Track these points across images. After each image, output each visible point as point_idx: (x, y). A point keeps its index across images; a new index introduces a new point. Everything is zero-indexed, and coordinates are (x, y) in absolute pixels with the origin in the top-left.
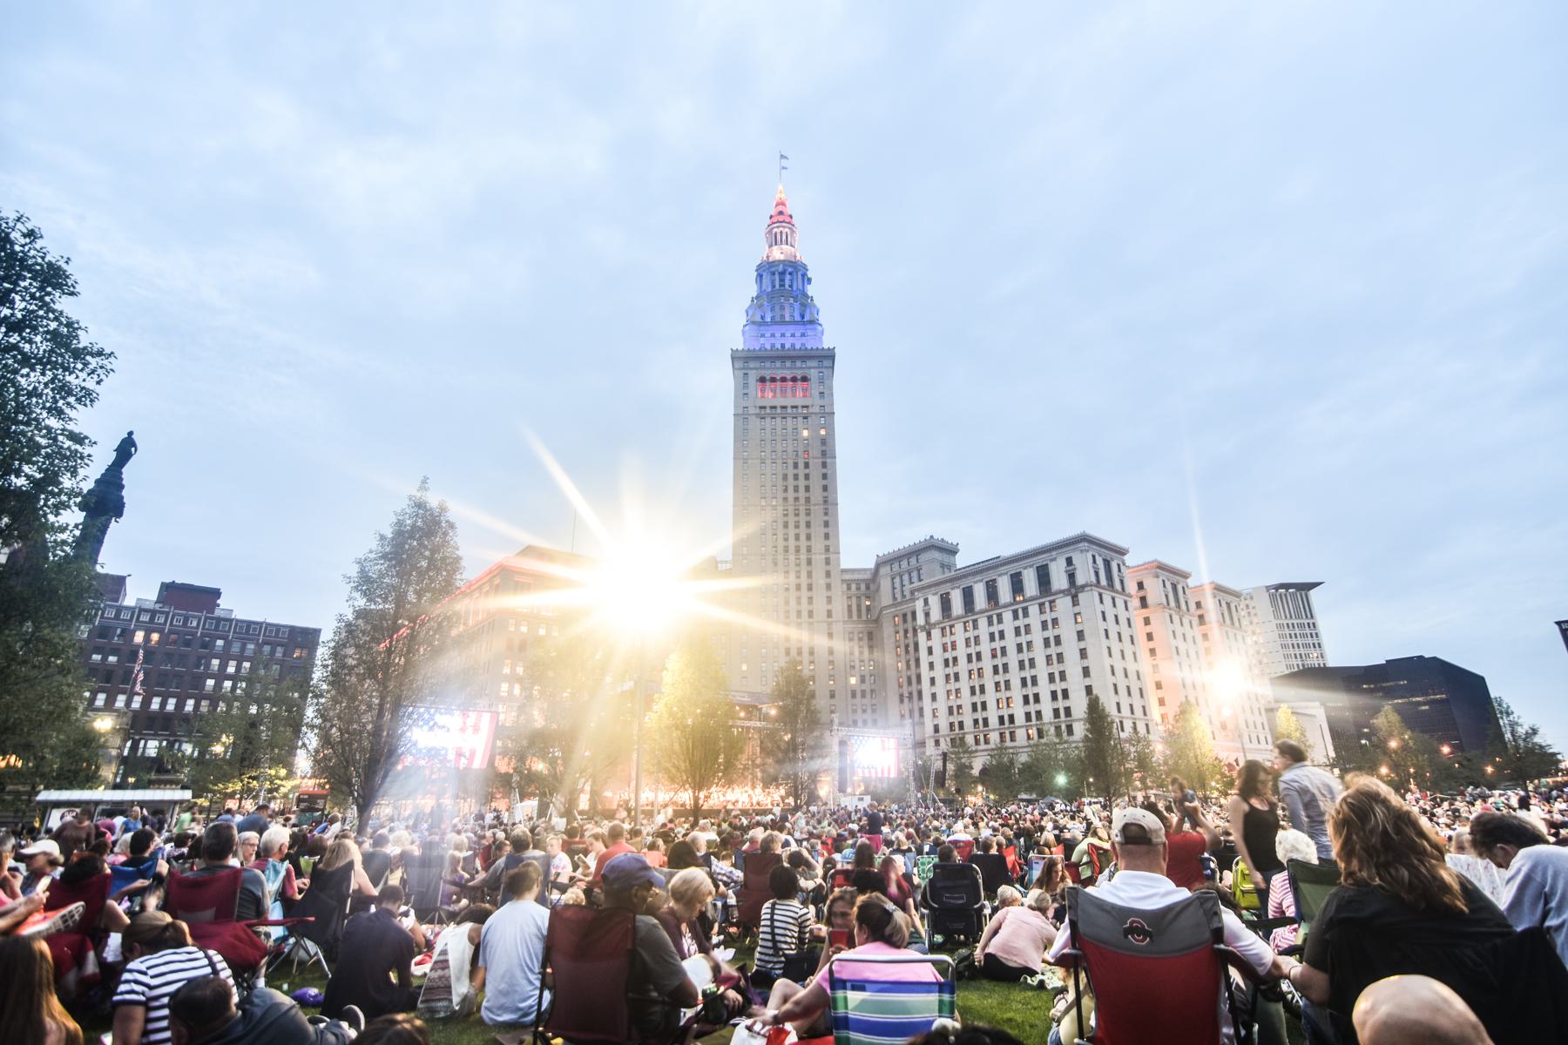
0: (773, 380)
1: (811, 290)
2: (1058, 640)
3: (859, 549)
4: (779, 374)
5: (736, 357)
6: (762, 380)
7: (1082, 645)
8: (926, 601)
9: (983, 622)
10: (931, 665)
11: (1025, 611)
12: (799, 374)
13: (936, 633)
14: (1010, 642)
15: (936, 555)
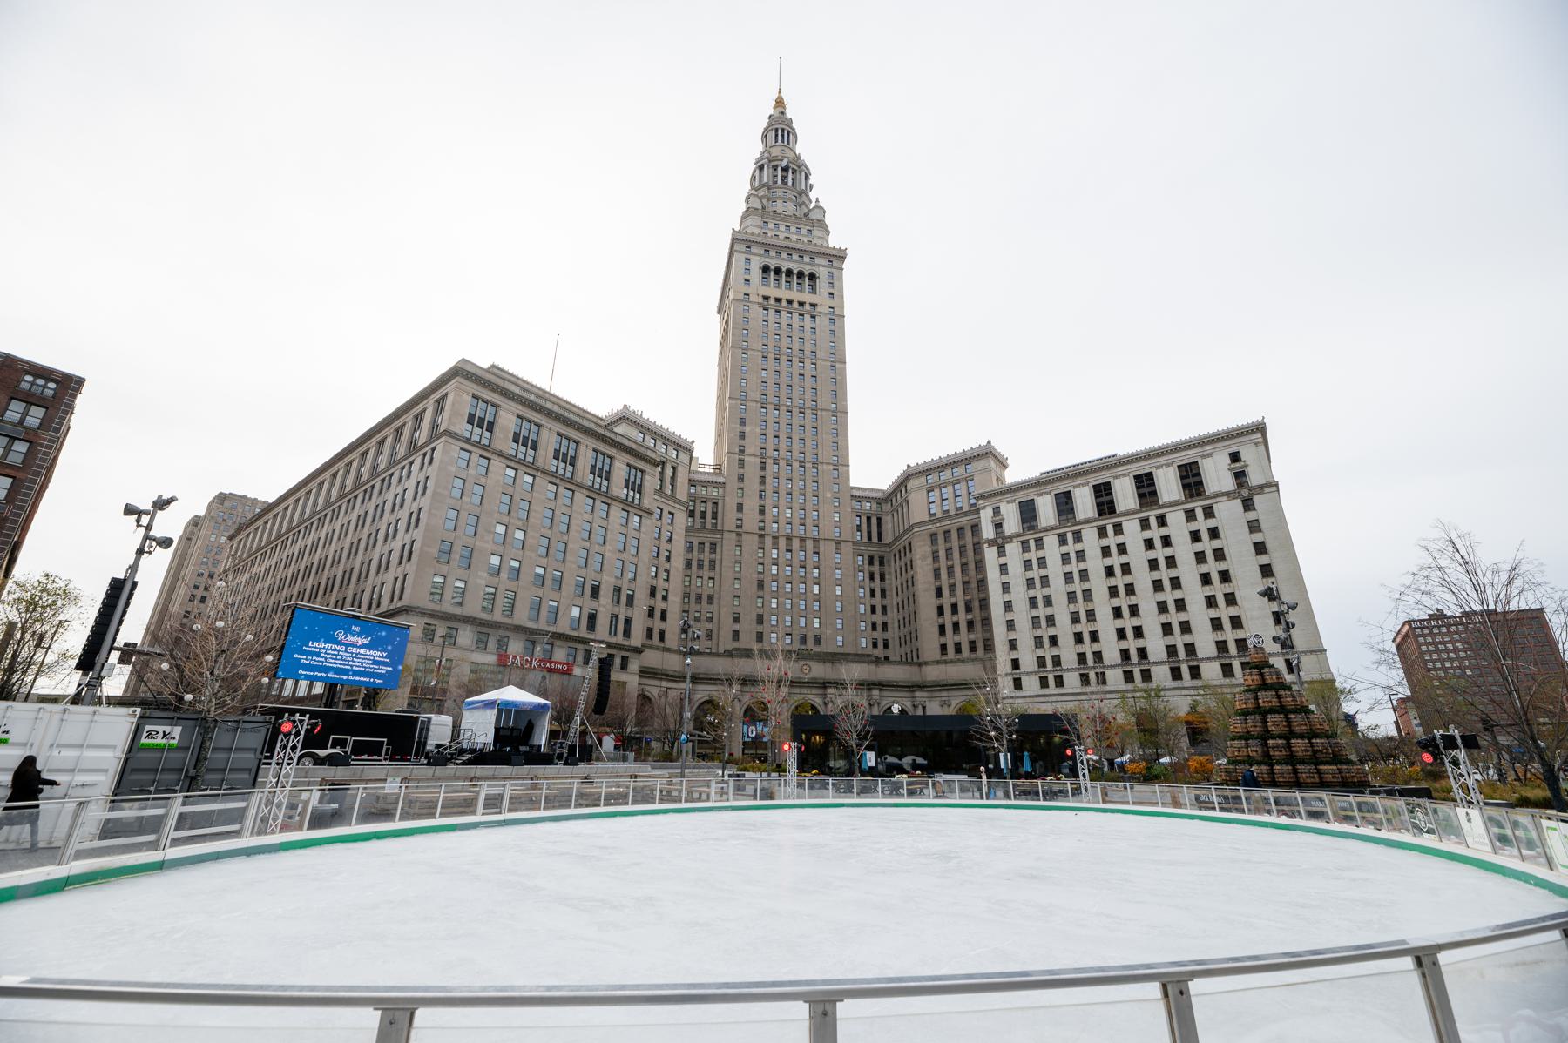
0: (778, 271)
1: (813, 195)
2: (1219, 555)
3: (873, 465)
4: (784, 266)
5: (734, 240)
6: (766, 269)
7: (1264, 560)
8: (996, 511)
9: (1090, 534)
10: (1006, 588)
11: (1162, 521)
12: (807, 270)
13: (1013, 549)
14: (1137, 556)
15: (992, 464)
